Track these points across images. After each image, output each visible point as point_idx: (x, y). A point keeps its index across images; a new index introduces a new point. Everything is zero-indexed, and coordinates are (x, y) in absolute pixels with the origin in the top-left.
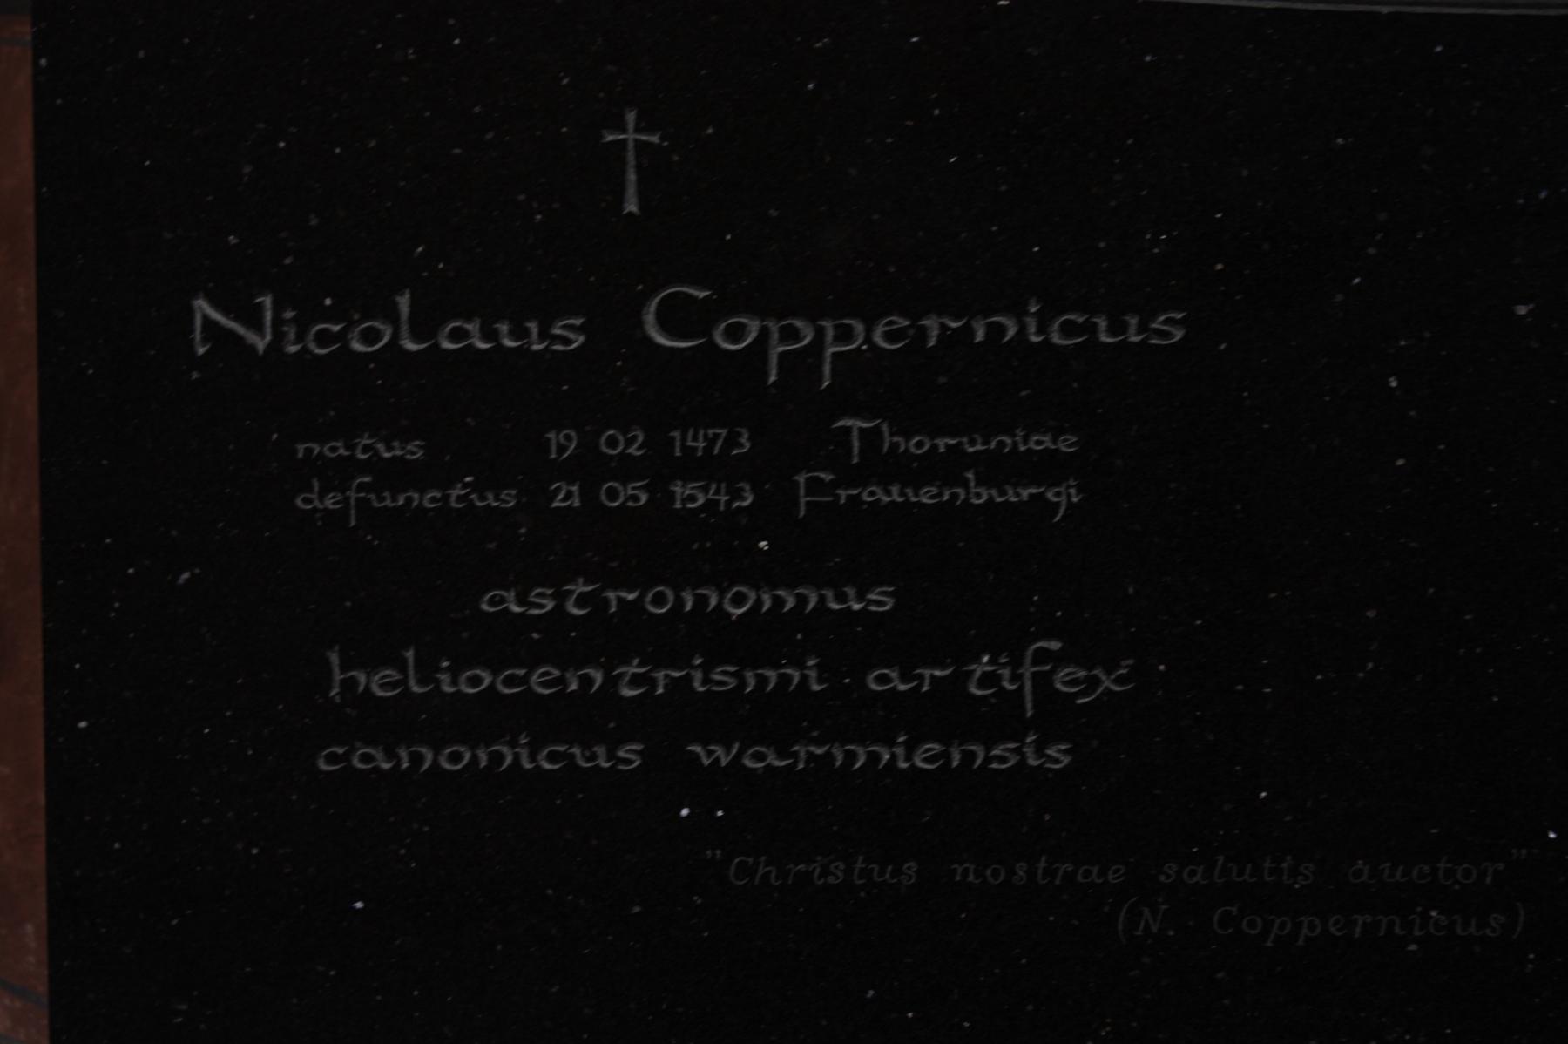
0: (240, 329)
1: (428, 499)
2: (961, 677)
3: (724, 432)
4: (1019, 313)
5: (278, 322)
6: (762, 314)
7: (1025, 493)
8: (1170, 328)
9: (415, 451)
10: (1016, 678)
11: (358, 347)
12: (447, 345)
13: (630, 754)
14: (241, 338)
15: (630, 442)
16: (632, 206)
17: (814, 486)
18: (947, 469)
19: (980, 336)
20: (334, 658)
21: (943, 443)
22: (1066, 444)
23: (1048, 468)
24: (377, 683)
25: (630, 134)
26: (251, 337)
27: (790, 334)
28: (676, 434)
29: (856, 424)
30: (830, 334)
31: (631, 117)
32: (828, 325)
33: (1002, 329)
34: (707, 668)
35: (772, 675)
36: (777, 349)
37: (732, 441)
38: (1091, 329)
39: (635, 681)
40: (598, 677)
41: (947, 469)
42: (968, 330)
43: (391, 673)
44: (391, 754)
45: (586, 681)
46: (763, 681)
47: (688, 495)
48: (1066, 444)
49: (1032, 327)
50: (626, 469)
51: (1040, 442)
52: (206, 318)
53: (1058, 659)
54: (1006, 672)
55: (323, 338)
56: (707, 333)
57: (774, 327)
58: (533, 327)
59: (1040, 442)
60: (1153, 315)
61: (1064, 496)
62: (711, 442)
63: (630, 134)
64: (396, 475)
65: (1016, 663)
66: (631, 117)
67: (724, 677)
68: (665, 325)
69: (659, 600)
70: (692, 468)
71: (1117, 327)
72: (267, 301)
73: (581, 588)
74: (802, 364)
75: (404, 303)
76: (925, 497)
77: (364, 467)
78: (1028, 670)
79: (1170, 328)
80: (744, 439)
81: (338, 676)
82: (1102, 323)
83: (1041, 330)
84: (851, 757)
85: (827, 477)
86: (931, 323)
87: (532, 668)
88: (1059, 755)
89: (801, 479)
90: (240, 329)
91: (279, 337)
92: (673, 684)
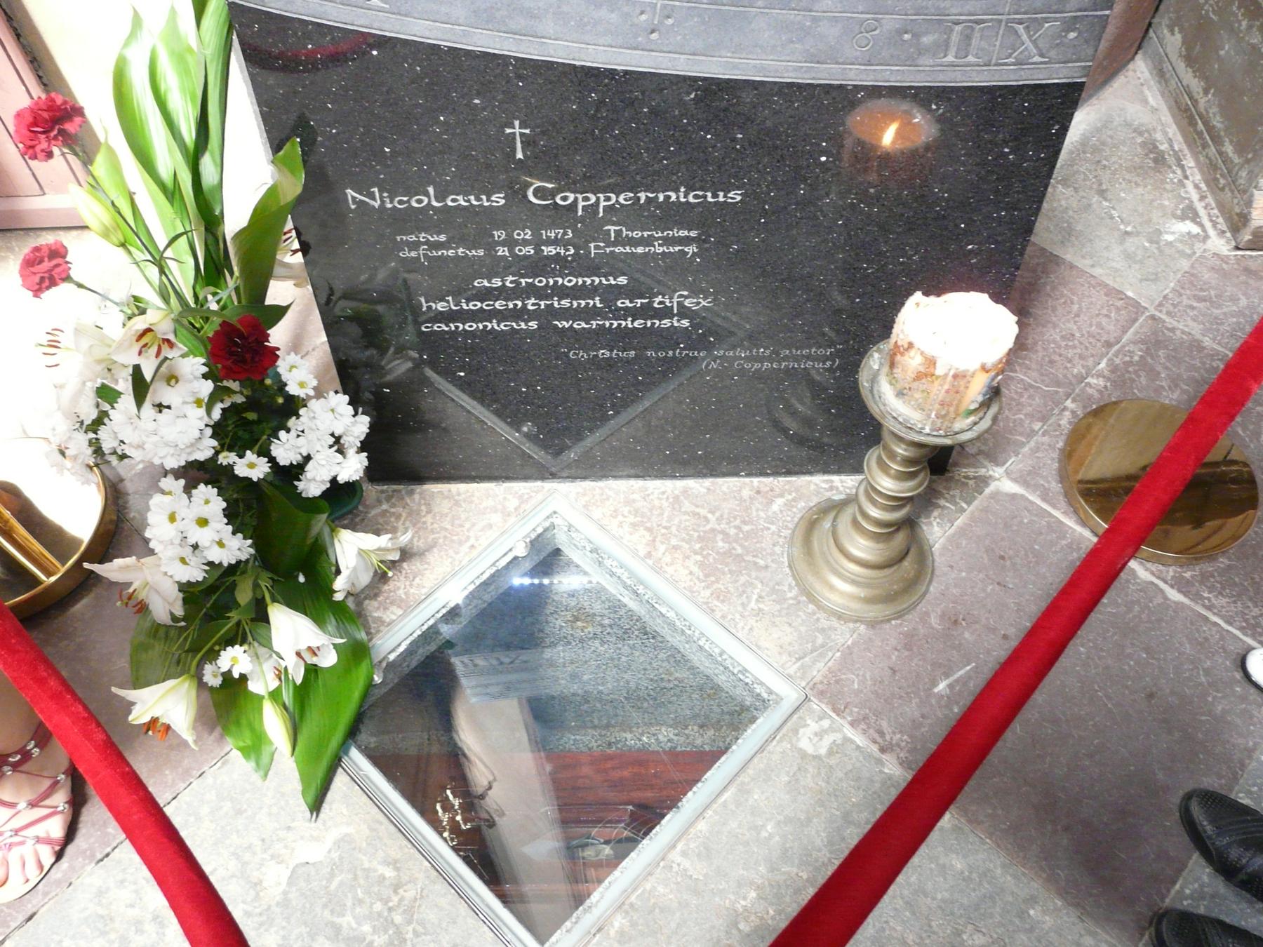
1: (451, 253)
2: (651, 303)
3: (562, 231)
4: (677, 190)
5: (381, 198)
6: (574, 192)
7: (677, 249)
8: (735, 196)
9: (443, 238)
11: (415, 204)
12: (450, 204)
13: (533, 325)
14: (367, 203)
15: (525, 234)
16: (520, 155)
18: (648, 242)
20: (423, 300)
21: (645, 234)
22: (693, 234)
23: (687, 241)
24: (440, 306)
25: (517, 129)
26: (372, 202)
28: (544, 232)
29: (612, 228)
31: (517, 123)
33: (669, 197)
34: (559, 301)
36: (581, 204)
37: (565, 233)
38: (705, 197)
39: (533, 305)
41: (648, 242)
42: (657, 197)
46: (579, 304)
48: (693, 234)
49: (682, 195)
50: (525, 243)
52: (352, 197)
53: (686, 297)
54: (668, 301)
55: (400, 202)
56: (553, 198)
57: (580, 197)
58: (484, 197)
60: (730, 191)
61: (691, 249)
62: (557, 234)
63: (517, 129)
65: (671, 298)
66: (517, 123)
68: (535, 195)
69: (540, 281)
70: (549, 242)
71: (715, 196)
72: (376, 190)
73: (511, 278)
75: (431, 190)
76: (640, 250)
77: (424, 244)
78: (675, 300)
79: (735, 196)
81: (425, 305)
82: (709, 194)
83: (685, 197)
85: (602, 244)
86: (642, 196)
87: (495, 301)
88: (685, 323)
89: (592, 245)
91: (383, 202)
92: (546, 306)
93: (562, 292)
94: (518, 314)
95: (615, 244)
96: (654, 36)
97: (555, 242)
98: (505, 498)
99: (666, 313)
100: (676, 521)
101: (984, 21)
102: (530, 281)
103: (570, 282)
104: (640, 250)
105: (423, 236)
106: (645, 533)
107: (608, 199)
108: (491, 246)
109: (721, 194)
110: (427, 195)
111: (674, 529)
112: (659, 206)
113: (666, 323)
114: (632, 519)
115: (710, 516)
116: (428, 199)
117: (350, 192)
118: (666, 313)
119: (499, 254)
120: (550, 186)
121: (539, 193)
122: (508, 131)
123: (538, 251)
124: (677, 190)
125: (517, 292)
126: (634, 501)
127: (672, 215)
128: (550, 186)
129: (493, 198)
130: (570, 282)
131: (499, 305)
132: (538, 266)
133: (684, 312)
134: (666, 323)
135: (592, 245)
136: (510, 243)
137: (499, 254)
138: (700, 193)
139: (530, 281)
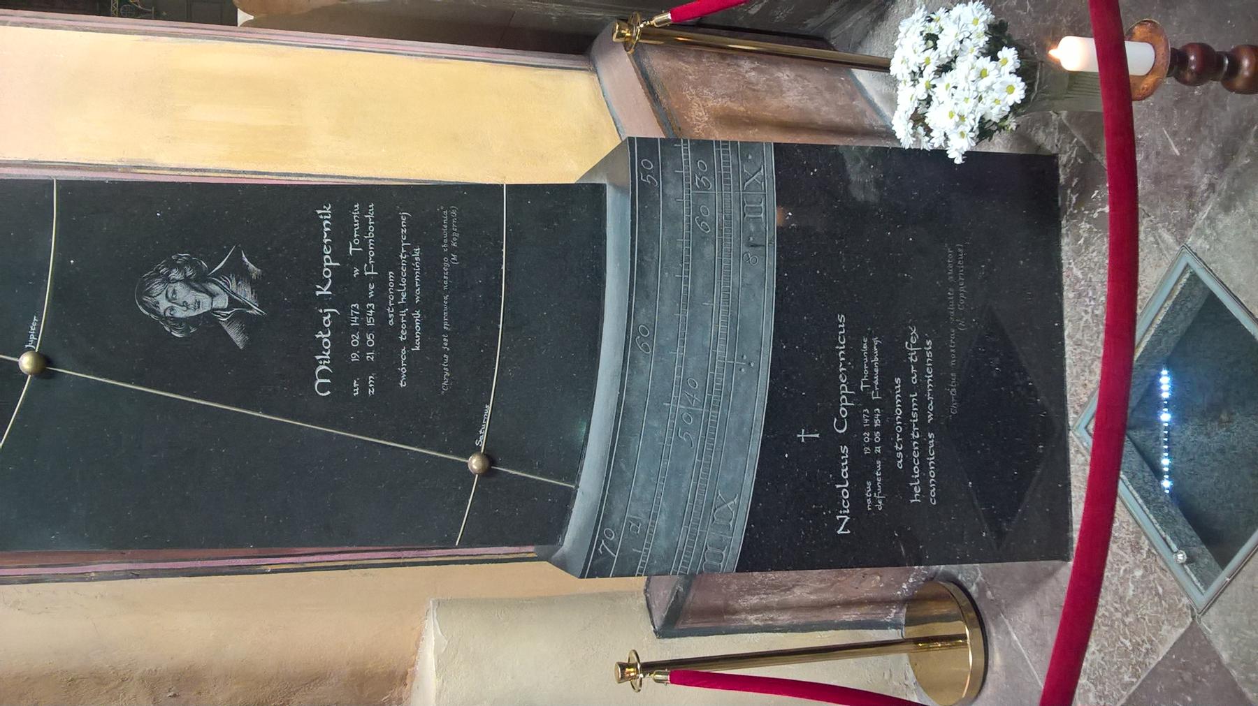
0: (844, 523)
1: (879, 480)
3: (864, 415)
4: (839, 350)
7: (875, 349)
8: (842, 318)
9: (869, 483)
10: (913, 351)
12: (847, 477)
13: (931, 435)
16: (817, 436)
17: (875, 395)
19: (843, 359)
21: (866, 367)
22: (865, 340)
23: (870, 345)
24: (917, 491)
26: (846, 521)
27: (844, 400)
30: (844, 392)
31: (799, 436)
32: (842, 392)
35: (914, 404)
36: (847, 404)
37: (865, 413)
38: (842, 334)
39: (916, 434)
40: (915, 443)
42: (842, 361)
43: (915, 488)
44: (932, 488)
45: (916, 445)
46: (915, 407)
47: (877, 423)
48: (865, 340)
49: (841, 348)
50: (872, 436)
53: (910, 343)
54: (912, 354)
55: (846, 504)
56: (843, 418)
58: (843, 457)
60: (839, 321)
61: (876, 341)
64: (874, 489)
65: (910, 351)
66: (799, 436)
67: (914, 415)
68: (842, 428)
69: (899, 429)
70: (872, 422)
72: (838, 517)
74: (850, 398)
75: (838, 486)
76: (877, 371)
77: (873, 495)
78: (912, 349)
79: (842, 318)
80: (865, 410)
81: (916, 500)
82: (840, 332)
83: (842, 345)
84: (930, 387)
86: (841, 370)
87: (913, 457)
89: (873, 398)
90: (844, 523)
91: (846, 514)
93: (906, 416)
94: (923, 445)
95: (873, 385)
96: (752, 365)
97: (872, 419)
98: (1078, 464)
99: (922, 355)
100: (1087, 342)
101: (743, 202)
102: (898, 435)
103: (899, 412)
104: (877, 371)
106: (1095, 364)
107: (844, 388)
108: (875, 456)
109: (840, 326)
111: (1092, 345)
112: (848, 360)
114: (1087, 374)
115: (1084, 319)
116: (844, 489)
118: (922, 355)
119: (879, 451)
120: (836, 420)
122: (803, 441)
123: (877, 429)
125: (907, 441)
126: (1077, 372)
127: (853, 353)
128: (836, 420)
129: (843, 452)
130: (899, 412)
132: (887, 431)
133: (921, 343)
135: (873, 398)
136: (872, 445)
137: (879, 451)
138: (840, 337)
139: (898, 435)
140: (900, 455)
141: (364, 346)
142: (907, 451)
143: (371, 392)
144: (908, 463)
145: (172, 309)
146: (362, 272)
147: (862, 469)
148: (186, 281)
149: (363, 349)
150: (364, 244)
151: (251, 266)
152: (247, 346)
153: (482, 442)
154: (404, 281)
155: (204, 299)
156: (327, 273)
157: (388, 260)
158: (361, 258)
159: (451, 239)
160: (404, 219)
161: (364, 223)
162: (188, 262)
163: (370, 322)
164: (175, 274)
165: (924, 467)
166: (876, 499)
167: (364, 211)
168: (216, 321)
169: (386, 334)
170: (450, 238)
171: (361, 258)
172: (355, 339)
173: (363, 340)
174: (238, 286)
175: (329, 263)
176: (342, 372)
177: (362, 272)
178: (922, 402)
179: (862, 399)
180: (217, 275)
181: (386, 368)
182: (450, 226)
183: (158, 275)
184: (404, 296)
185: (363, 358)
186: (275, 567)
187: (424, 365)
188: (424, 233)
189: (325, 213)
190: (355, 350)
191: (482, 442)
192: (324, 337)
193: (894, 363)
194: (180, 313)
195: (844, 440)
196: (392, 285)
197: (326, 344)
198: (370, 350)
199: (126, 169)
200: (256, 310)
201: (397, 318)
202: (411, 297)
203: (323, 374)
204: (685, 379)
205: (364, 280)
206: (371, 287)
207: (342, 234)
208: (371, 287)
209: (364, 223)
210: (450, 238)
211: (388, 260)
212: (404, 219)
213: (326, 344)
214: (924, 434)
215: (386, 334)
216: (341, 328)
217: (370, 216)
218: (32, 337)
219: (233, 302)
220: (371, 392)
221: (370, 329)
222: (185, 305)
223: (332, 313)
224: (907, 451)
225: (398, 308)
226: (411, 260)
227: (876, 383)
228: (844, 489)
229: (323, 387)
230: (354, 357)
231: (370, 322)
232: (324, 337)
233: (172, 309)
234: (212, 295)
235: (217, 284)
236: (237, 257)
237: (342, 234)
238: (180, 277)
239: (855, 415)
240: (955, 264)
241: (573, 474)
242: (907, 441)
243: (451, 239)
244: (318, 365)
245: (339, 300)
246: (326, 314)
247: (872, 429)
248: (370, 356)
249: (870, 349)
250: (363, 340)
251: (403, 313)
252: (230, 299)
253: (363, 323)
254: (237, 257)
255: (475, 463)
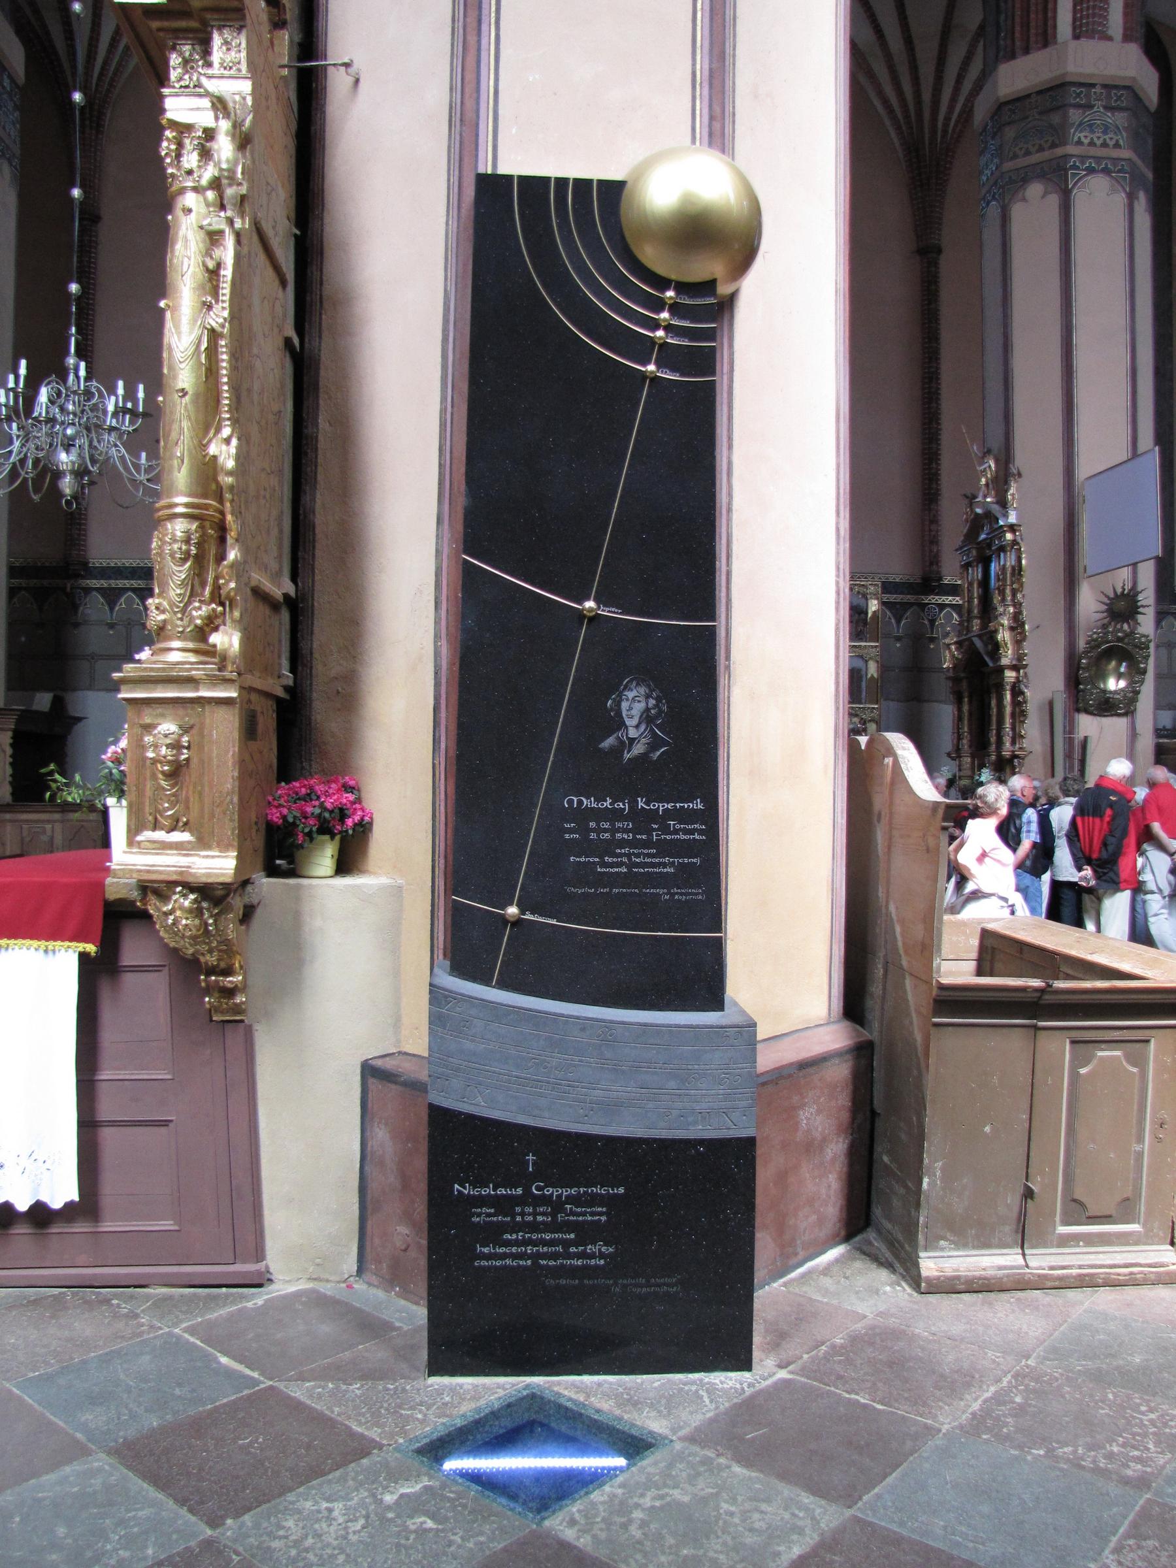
1: (495, 1219)
2: (586, 1249)
4: (596, 1187)
8: (621, 1190)
9: (493, 1211)
13: (529, 1262)
18: (584, 1214)
22: (604, 1209)
23: (601, 1214)
24: (486, 1250)
25: (531, 1157)
29: (568, 1206)
36: (555, 1193)
41: (584, 1214)
47: (540, 1218)
48: (604, 1209)
51: (600, 1209)
59: (600, 1209)
61: (603, 1218)
63: (531, 1157)
64: (489, 1215)
67: (545, 1249)
74: (559, 1196)
76: (581, 1218)
79: (621, 1190)
88: (602, 1262)
97: (543, 1214)
99: (592, 1256)
103: (548, 1236)
104: (581, 1218)
105: (484, 1210)
108: (513, 1216)
110: (489, 1188)
112: (589, 1195)
113: (593, 1262)
116: (488, 1191)
117: (456, 1186)
118: (592, 1256)
121: (538, 1188)
124: (596, 1187)
125: (525, 1243)
127: (593, 1200)
130: (548, 1236)
131: (514, 1250)
132: (534, 1227)
133: (602, 1256)
134: (593, 1262)
136: (523, 1214)
140: (514, 1236)
141: (600, 832)
142: (517, 1243)
143: (567, 836)
144: (508, 1244)
145: (627, 700)
146: (655, 830)
147: (503, 1205)
148: (647, 710)
149: (599, 831)
150: (676, 832)
151: (658, 753)
152: (601, 750)
153: (528, 916)
154: (649, 860)
155: (635, 722)
156: (654, 806)
157: (665, 848)
158: (665, 829)
159: (680, 894)
160: (695, 860)
161: (691, 832)
162: (660, 712)
163: (618, 836)
164: (652, 702)
165: (504, 1256)
166: (482, 1216)
167: (701, 832)
168: (619, 729)
169: (608, 848)
170: (681, 894)
171: (665, 829)
172: (606, 825)
173: (605, 830)
174: (645, 744)
175: (662, 807)
176: (582, 816)
177: (655, 830)
178: (554, 1256)
179: (557, 1206)
180: (652, 730)
181: (585, 847)
182: (690, 894)
183: (652, 691)
184: (637, 860)
185: (593, 830)
186: (437, 766)
187: (585, 875)
188: (686, 876)
189: (698, 805)
190: (598, 825)
191: (528, 916)
192: (607, 803)
193: (586, 1233)
194: (625, 705)
195: (527, 1191)
196: (646, 851)
197: (602, 805)
198: (598, 836)
199: (728, 668)
200: (627, 756)
201: (621, 855)
202: (638, 865)
203: (580, 802)
204: (575, 1066)
205: (649, 832)
206: (644, 837)
207: (683, 816)
208: (644, 837)
209: (691, 832)
210: (681, 894)
211: (665, 848)
212: (695, 860)
213: (602, 805)
214: (530, 1257)
215: (608, 848)
216: (616, 815)
217: (697, 837)
218: (607, 609)
219: (632, 741)
220: (567, 836)
221: (613, 835)
222: (630, 709)
223: (625, 809)
224: (517, 1243)
225: (629, 856)
226: (664, 865)
227: (571, 1218)
228: (488, 1191)
229: (571, 802)
230: (592, 824)
231: (618, 836)
232: (607, 803)
233: (627, 700)
234: (637, 727)
235: (645, 730)
236: (665, 743)
237: (683, 816)
238: (650, 705)
239: (546, 1200)
240: (664, 1284)
241: (503, 985)
242: (525, 1243)
243: (680, 894)
244: (587, 799)
245: (635, 813)
246: (624, 805)
247: (535, 1214)
248: (593, 836)
249: (598, 1215)
250: (605, 830)
251: (625, 860)
252: (634, 739)
253: (618, 830)
254: (665, 743)
255: (513, 910)
